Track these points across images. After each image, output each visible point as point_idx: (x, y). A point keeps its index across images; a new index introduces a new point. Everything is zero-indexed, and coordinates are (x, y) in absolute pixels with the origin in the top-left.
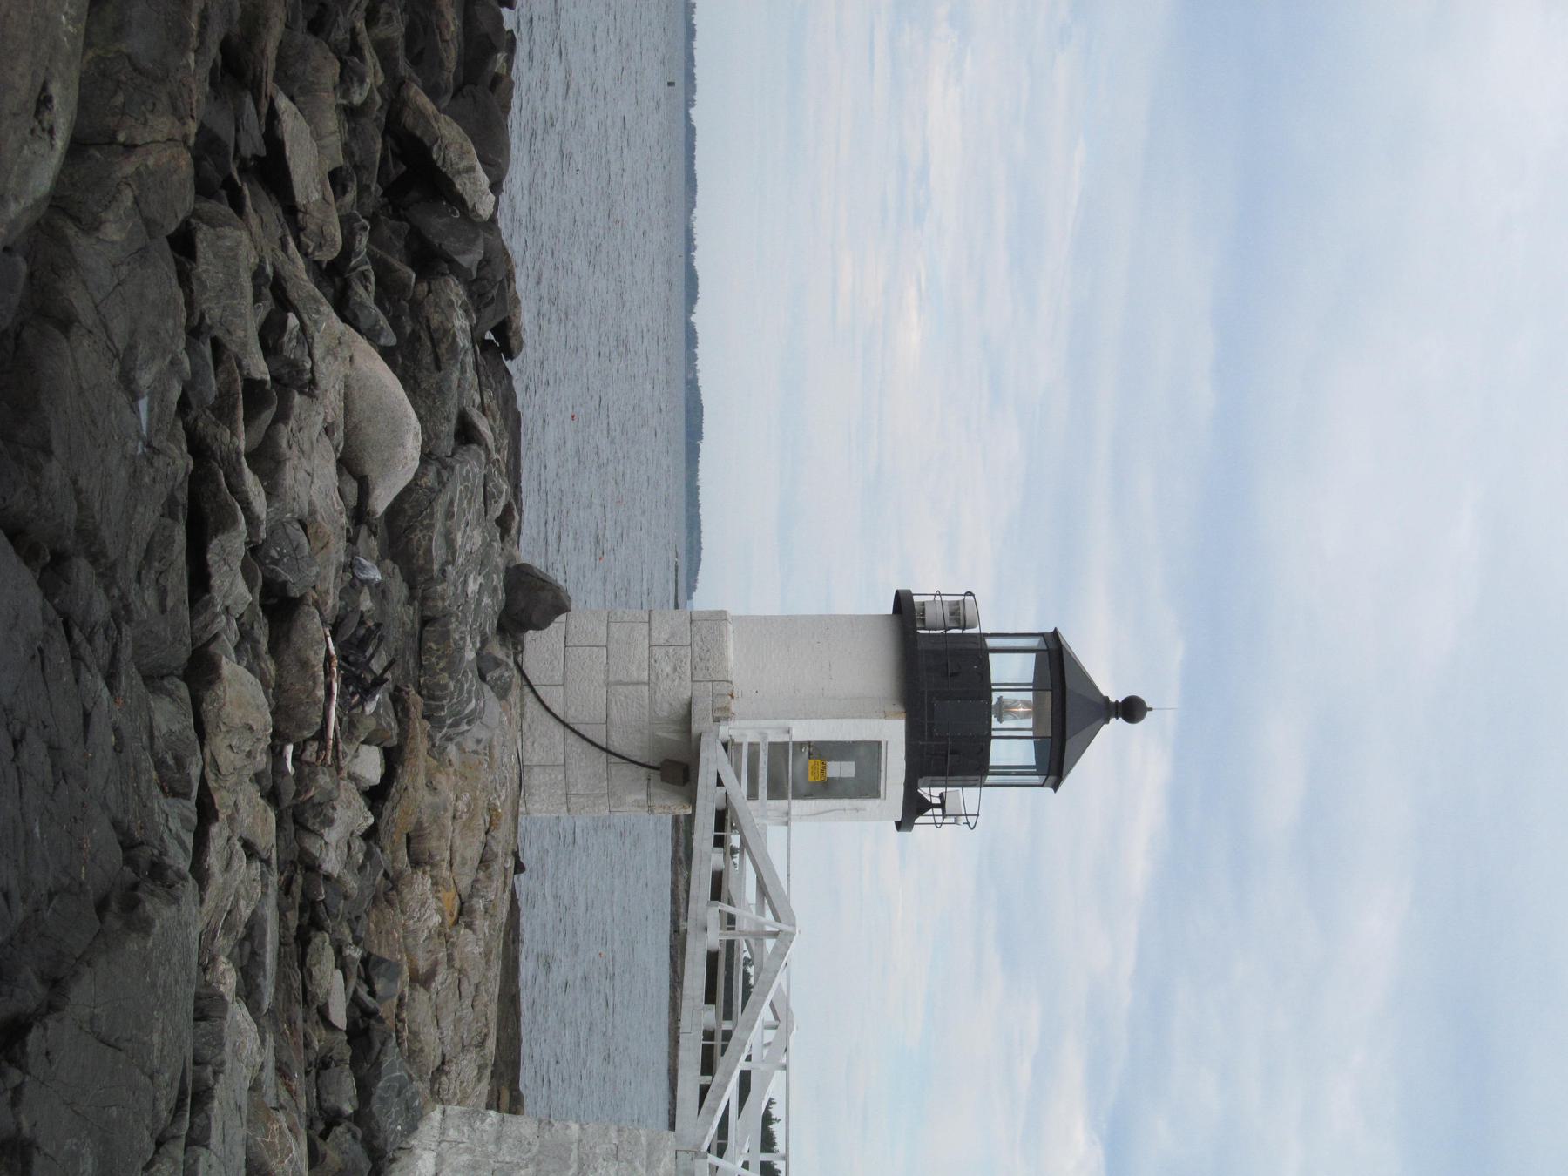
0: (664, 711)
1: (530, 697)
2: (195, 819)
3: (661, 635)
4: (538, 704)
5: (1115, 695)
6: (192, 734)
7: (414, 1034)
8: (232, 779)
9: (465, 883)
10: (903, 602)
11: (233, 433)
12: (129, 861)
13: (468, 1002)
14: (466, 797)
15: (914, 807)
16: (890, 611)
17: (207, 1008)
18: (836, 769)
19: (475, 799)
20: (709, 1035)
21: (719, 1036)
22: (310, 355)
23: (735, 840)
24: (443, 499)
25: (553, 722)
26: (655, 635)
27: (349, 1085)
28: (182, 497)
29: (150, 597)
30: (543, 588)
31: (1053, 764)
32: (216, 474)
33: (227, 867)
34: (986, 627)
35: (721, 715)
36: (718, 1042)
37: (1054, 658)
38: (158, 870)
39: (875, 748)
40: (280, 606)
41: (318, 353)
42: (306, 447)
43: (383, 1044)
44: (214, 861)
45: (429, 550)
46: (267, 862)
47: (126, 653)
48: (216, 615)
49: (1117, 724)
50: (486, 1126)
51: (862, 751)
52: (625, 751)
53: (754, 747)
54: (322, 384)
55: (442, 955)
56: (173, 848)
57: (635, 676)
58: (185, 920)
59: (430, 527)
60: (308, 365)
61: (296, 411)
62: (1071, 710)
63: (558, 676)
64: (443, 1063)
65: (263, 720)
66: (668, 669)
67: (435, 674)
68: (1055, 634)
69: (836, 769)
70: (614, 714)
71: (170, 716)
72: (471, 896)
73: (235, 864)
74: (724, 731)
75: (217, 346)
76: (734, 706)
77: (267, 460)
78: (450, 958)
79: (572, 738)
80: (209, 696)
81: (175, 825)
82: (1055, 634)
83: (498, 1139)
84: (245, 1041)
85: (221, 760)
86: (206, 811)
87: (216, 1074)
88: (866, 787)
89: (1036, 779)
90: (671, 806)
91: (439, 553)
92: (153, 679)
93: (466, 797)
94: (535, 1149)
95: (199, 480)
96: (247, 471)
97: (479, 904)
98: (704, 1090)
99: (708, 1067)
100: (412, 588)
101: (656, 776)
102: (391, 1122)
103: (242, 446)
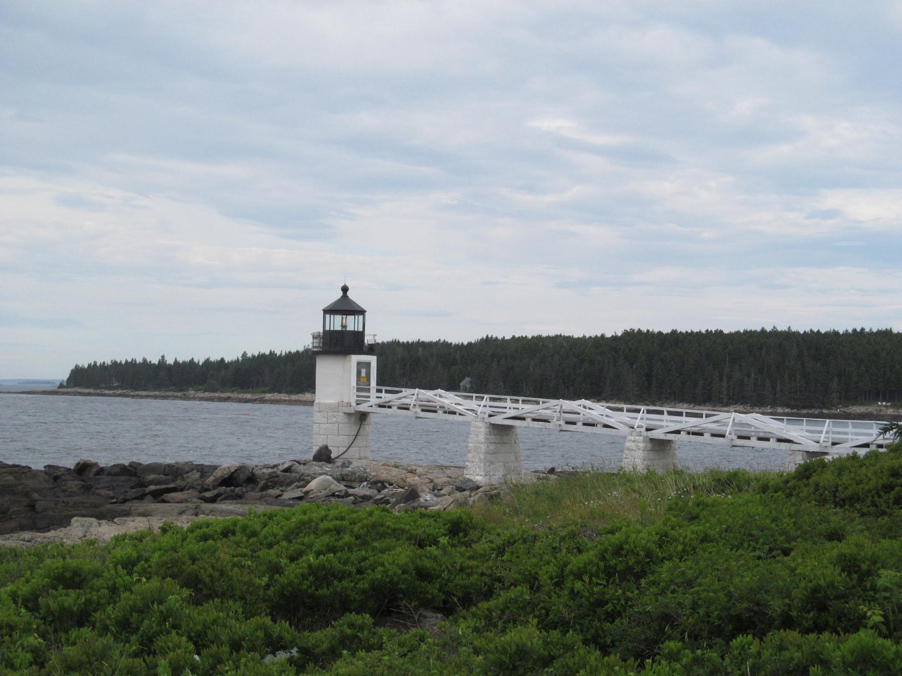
0: (346, 420)
3: (325, 420)
5: (341, 294)
9: (404, 471)
20: (445, 412)
23: (390, 404)
34: (321, 331)
35: (349, 405)
37: (330, 311)
39: (359, 364)
49: (349, 294)
53: (358, 396)
62: (345, 307)
74: (354, 404)
76: (346, 401)
88: (368, 365)
90: (372, 419)
98: (460, 414)
99: (454, 413)
102: (471, 485)
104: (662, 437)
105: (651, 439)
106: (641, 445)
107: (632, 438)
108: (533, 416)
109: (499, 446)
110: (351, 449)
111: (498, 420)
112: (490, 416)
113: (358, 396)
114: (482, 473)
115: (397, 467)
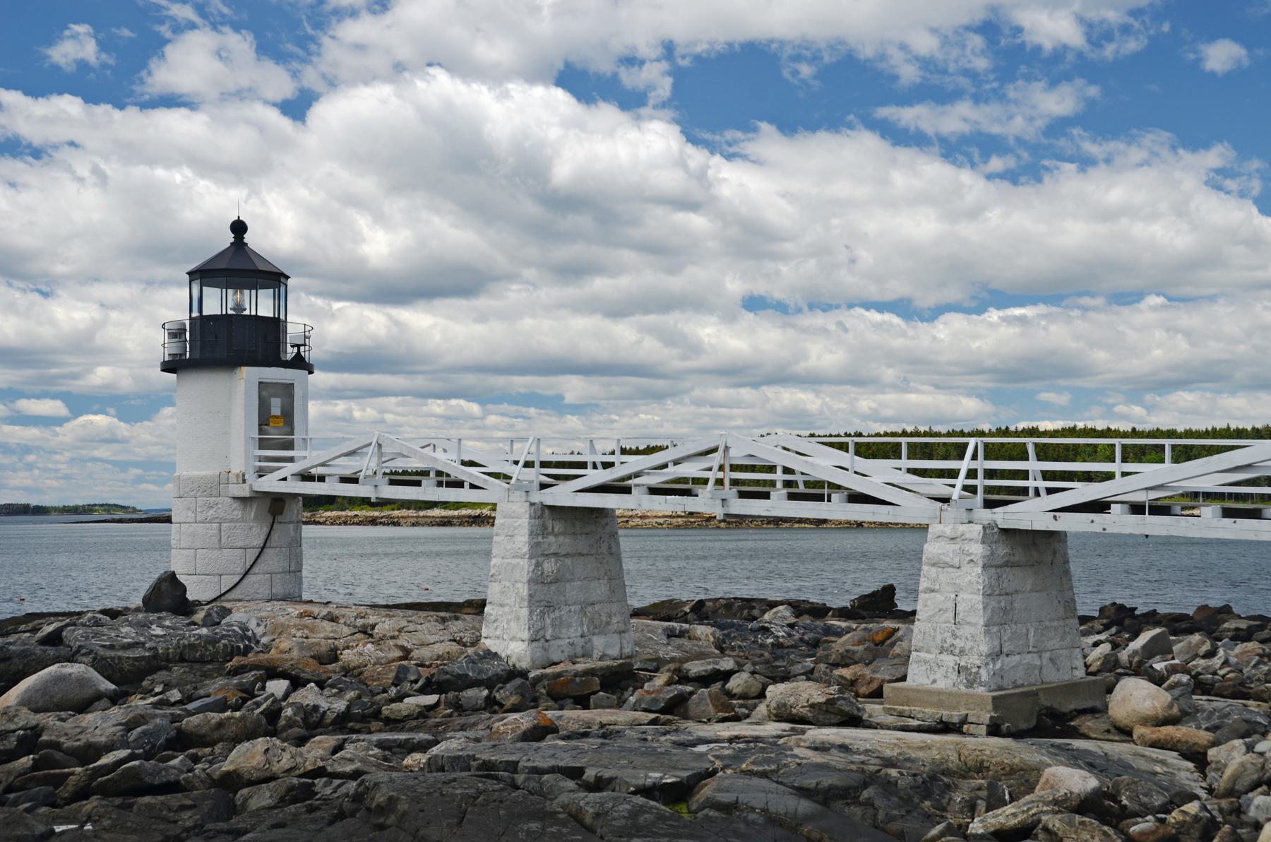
0: (238, 514)
1: (228, 596)
2: (324, 779)
4: (234, 591)
5: (230, 238)
6: (272, 784)
7: (439, 657)
8: (299, 760)
9: (346, 630)
10: (168, 367)
11: (72, 774)
12: (353, 815)
13: (419, 627)
14: (293, 631)
15: (300, 363)
16: (175, 375)
17: (436, 765)
18: (276, 410)
19: (295, 626)
20: (440, 484)
21: (440, 479)
22: (14, 731)
24: (102, 652)
25: (244, 581)
26: (189, 520)
27: (471, 693)
28: (118, 801)
29: (186, 815)
30: (159, 589)
31: (274, 279)
32: (101, 782)
33: (351, 760)
34: (185, 317)
36: (444, 479)
37: (204, 275)
38: (358, 798)
39: (262, 385)
40: (182, 741)
41: (13, 727)
42: (78, 730)
43: (447, 673)
44: (349, 768)
45: (135, 659)
46: (345, 740)
47: (222, 825)
48: (195, 776)
49: (248, 238)
50: (494, 613)
51: (264, 393)
52: (263, 538)
54: (34, 723)
55: (391, 642)
56: (343, 790)
57: (215, 532)
58: (384, 782)
59: (120, 658)
60: (22, 732)
61: (53, 738)
62: (237, 264)
63: (217, 579)
64: (454, 640)
65: (261, 743)
66: (212, 512)
67: (217, 652)
68: (189, 273)
69: (276, 410)
70: (240, 544)
71: (262, 798)
72: (355, 627)
73: (349, 756)
75: (9, 789)
77: (89, 753)
78: (392, 638)
79: (255, 570)
80: (246, 776)
81: (328, 791)
82: (189, 273)
83: (502, 606)
84: (452, 745)
85: (287, 767)
86: (319, 772)
87: (475, 760)
88: (288, 390)
89: (283, 289)
91: (138, 653)
92: (233, 810)
93: (293, 631)
94: (507, 584)
95: (104, 791)
96: (99, 763)
97: (360, 622)
98: (473, 486)
99: (459, 484)
100: (160, 668)
101: (279, 518)
102: (493, 668)
103: (78, 770)
104: (1044, 523)
105: (1009, 534)
106: (978, 550)
107: (948, 530)
108: (655, 480)
109: (568, 561)
110: (250, 578)
111: (564, 495)
112: (543, 486)
113: (261, 459)
114: (526, 635)
115: (333, 619)
